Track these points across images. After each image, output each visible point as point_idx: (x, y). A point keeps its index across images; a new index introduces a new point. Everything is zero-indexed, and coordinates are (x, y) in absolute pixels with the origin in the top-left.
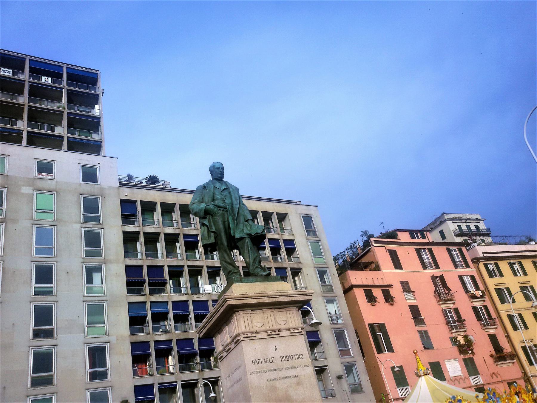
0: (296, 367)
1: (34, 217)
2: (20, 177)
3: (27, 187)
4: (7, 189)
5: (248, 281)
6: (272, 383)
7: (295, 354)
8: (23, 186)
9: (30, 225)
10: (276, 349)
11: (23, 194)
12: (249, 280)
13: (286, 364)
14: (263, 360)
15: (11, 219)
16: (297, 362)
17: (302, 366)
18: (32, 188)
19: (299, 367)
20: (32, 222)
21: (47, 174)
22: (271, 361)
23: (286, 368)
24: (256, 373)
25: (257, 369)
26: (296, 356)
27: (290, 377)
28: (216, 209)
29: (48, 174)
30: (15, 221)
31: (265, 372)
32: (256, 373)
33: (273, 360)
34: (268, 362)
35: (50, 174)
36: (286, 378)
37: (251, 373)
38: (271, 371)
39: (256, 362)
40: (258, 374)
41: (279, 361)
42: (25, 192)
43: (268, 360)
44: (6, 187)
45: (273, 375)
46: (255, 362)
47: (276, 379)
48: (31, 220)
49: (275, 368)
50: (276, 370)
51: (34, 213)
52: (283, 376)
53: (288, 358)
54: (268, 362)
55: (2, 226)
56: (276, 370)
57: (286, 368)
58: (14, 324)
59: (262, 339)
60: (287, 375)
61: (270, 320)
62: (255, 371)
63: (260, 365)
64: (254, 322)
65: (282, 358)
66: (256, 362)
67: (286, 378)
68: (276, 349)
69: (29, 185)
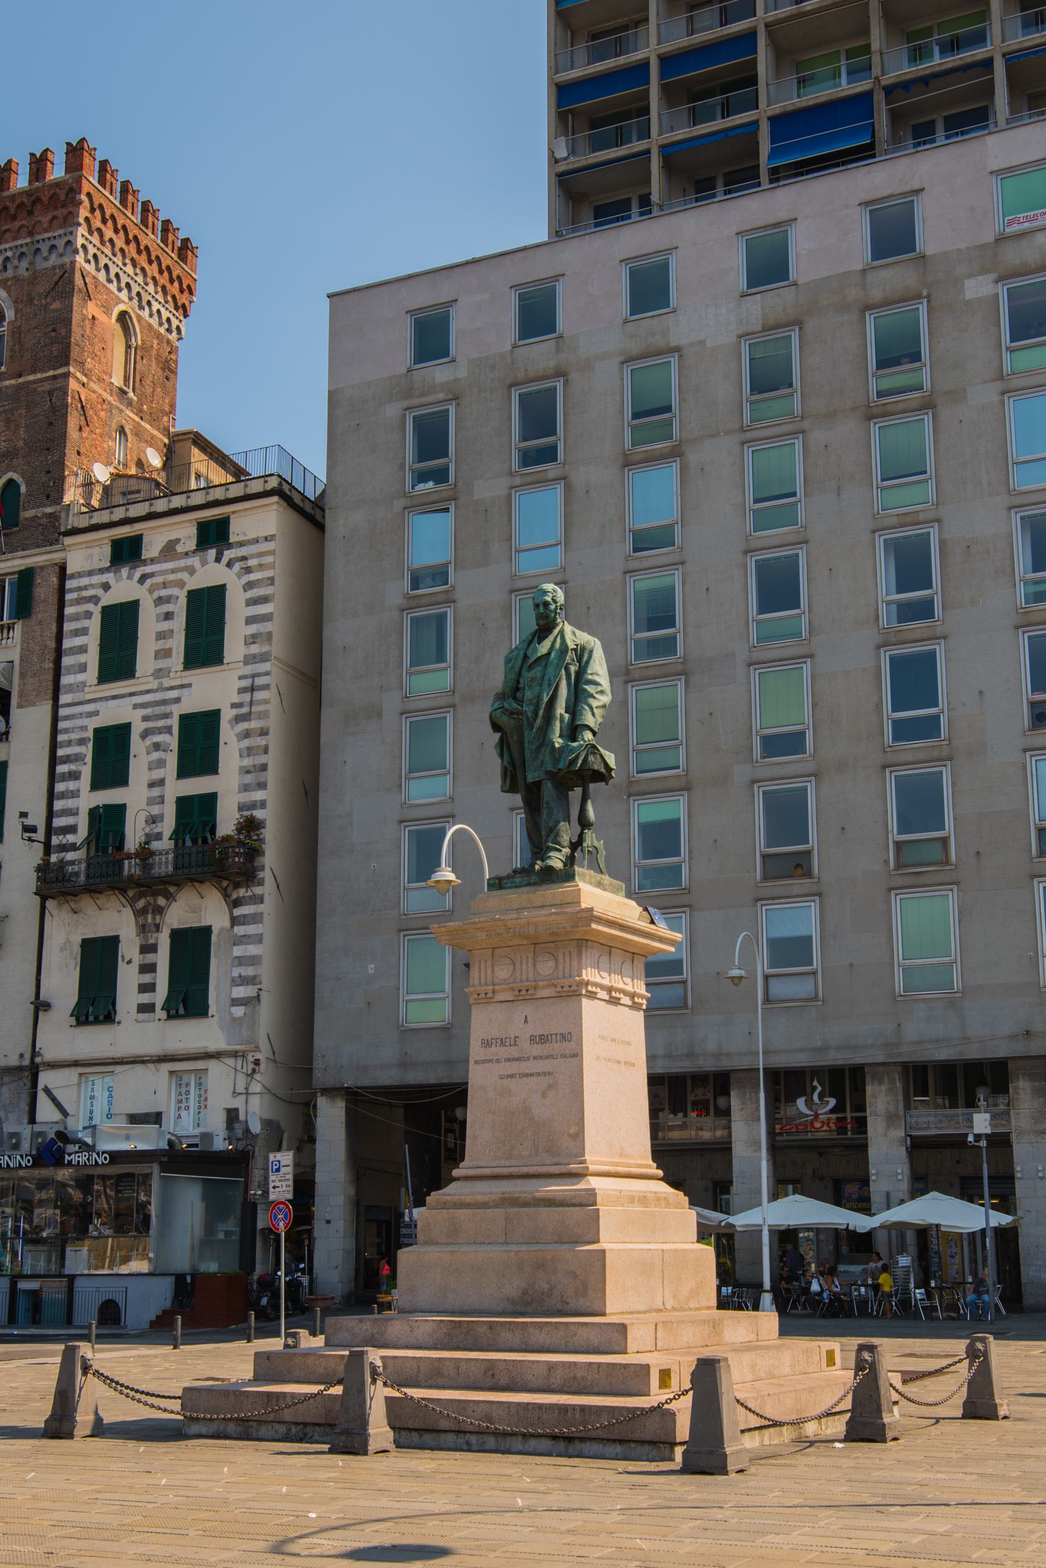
0: (551, 1057)
1: (1007, 369)
2: (958, 250)
3: (980, 278)
4: (928, 301)
5: (513, 885)
6: (505, 1081)
7: (557, 1032)
8: (970, 276)
9: (995, 398)
10: (526, 1021)
11: (968, 303)
12: (514, 882)
13: (537, 1050)
14: (499, 1041)
15: (946, 393)
16: (557, 1047)
17: (564, 1056)
18: (993, 276)
19: (559, 1056)
20: (999, 386)
21: (1032, 213)
22: (512, 1043)
23: (535, 1058)
24: (484, 1062)
25: (486, 1055)
26: (558, 1037)
27: (539, 1074)
28: (505, 718)
29: (1036, 212)
30: (957, 396)
31: (498, 1061)
32: (484, 1062)
33: (515, 1041)
34: (508, 1044)
35: (1040, 211)
36: (531, 1075)
37: (476, 1062)
38: (509, 1060)
39: (488, 1044)
40: (486, 1065)
41: (525, 1045)
42: (975, 296)
43: (508, 1040)
44: (925, 292)
45: (514, 1068)
46: (487, 1044)
47: (512, 1076)
48: (998, 380)
49: (517, 1055)
50: (518, 1059)
51: (1006, 356)
52: (527, 1071)
53: (543, 1039)
54: (508, 1044)
55: (926, 417)
56: (518, 1059)
57: (535, 1058)
58: (981, 691)
59: (506, 1004)
60: (533, 1071)
61: (524, 966)
62: (483, 1058)
63: (493, 1049)
64: (496, 969)
65: (533, 1039)
66: (488, 1044)
67: (531, 1075)
68: (526, 1021)
69: (984, 271)
